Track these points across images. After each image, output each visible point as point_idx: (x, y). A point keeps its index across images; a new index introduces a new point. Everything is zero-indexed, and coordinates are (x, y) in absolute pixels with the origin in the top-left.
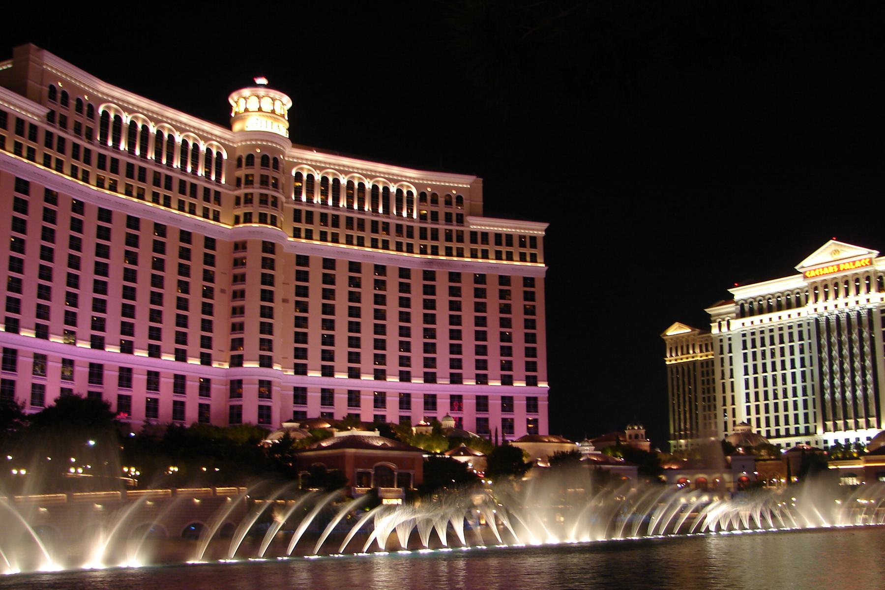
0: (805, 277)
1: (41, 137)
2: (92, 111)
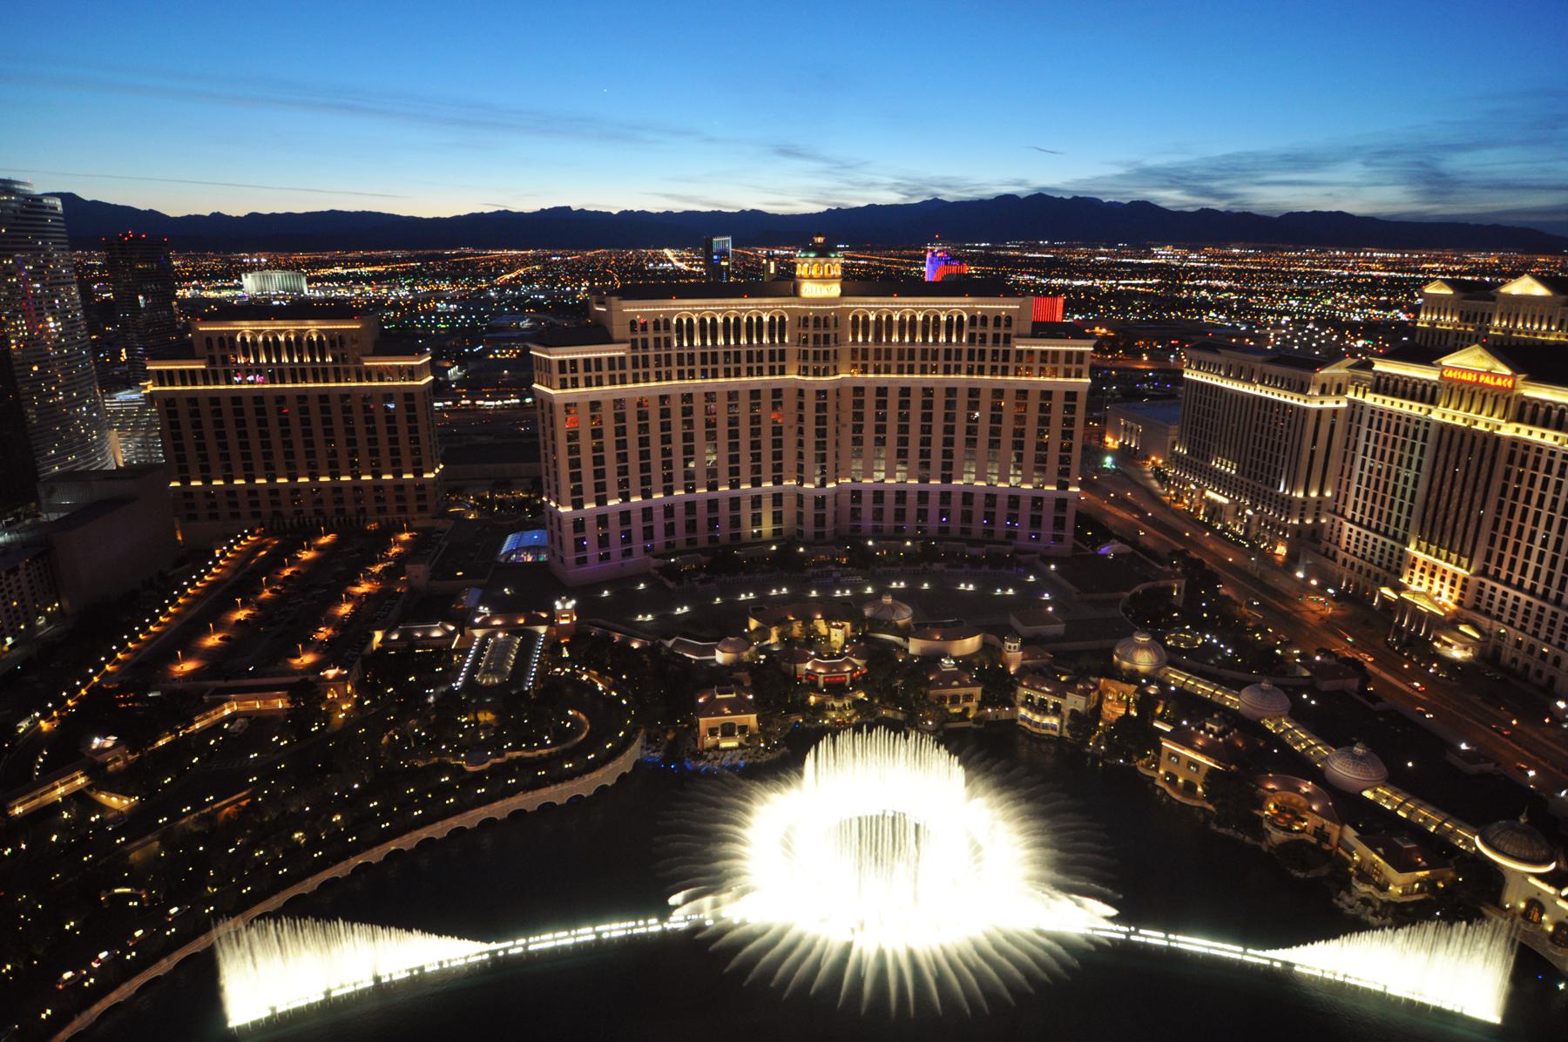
1: (629, 363)
2: (667, 322)
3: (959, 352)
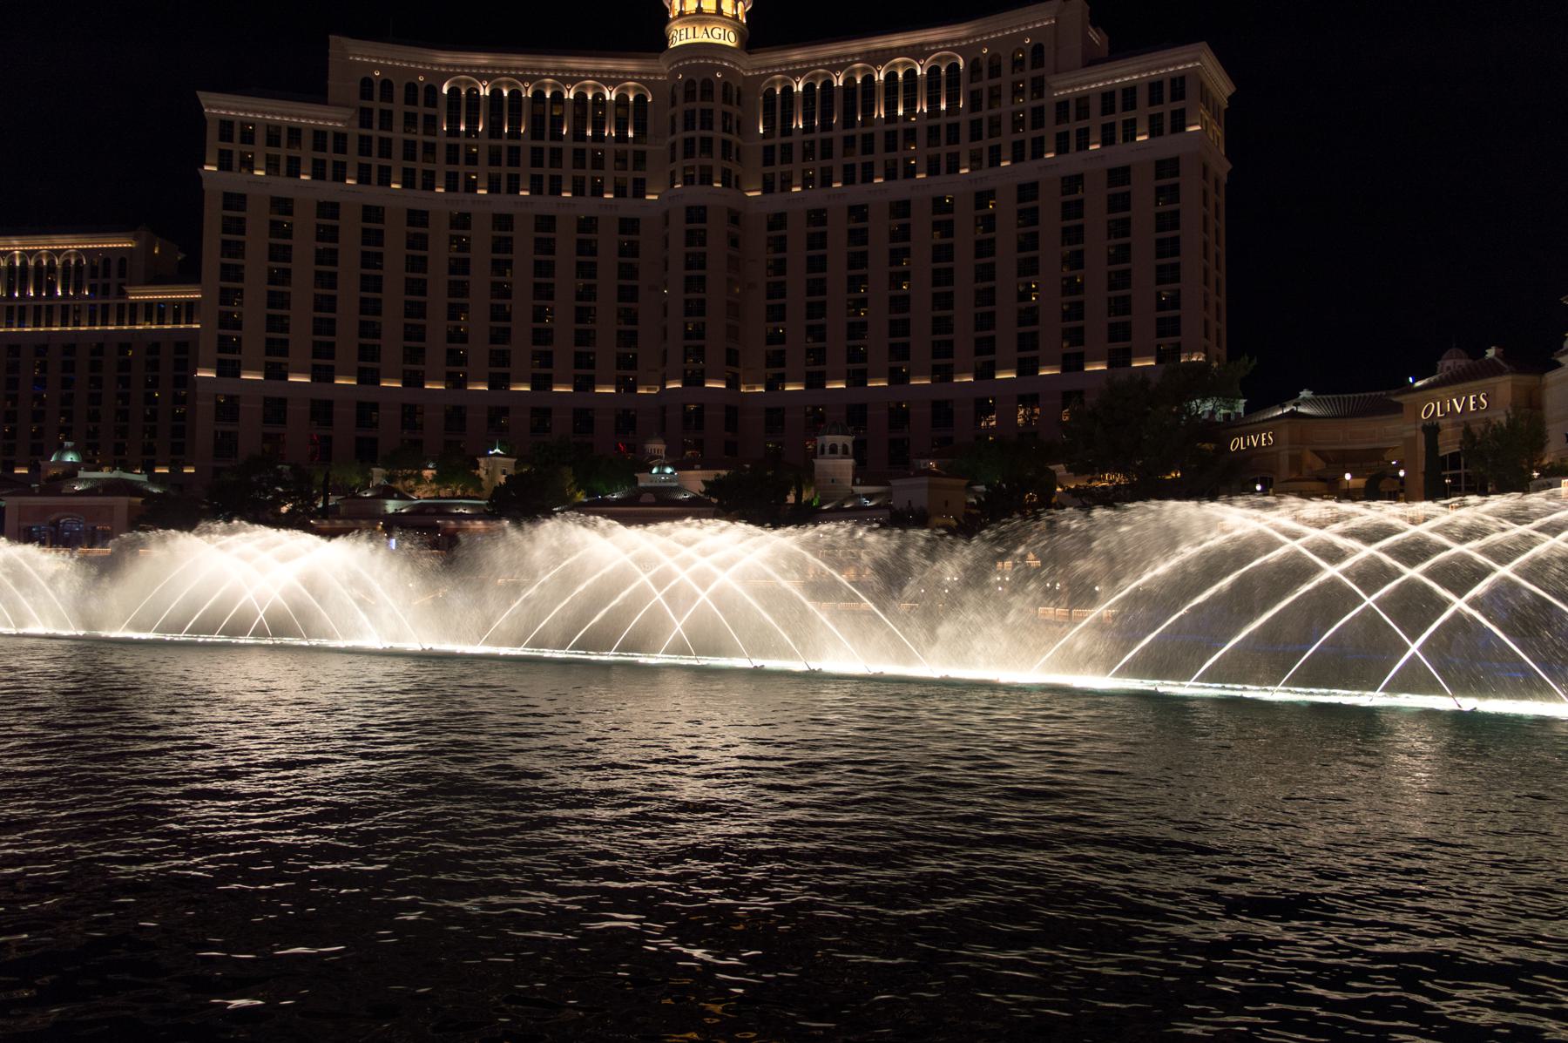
1: (353, 146)
2: (433, 91)
3: (953, 129)
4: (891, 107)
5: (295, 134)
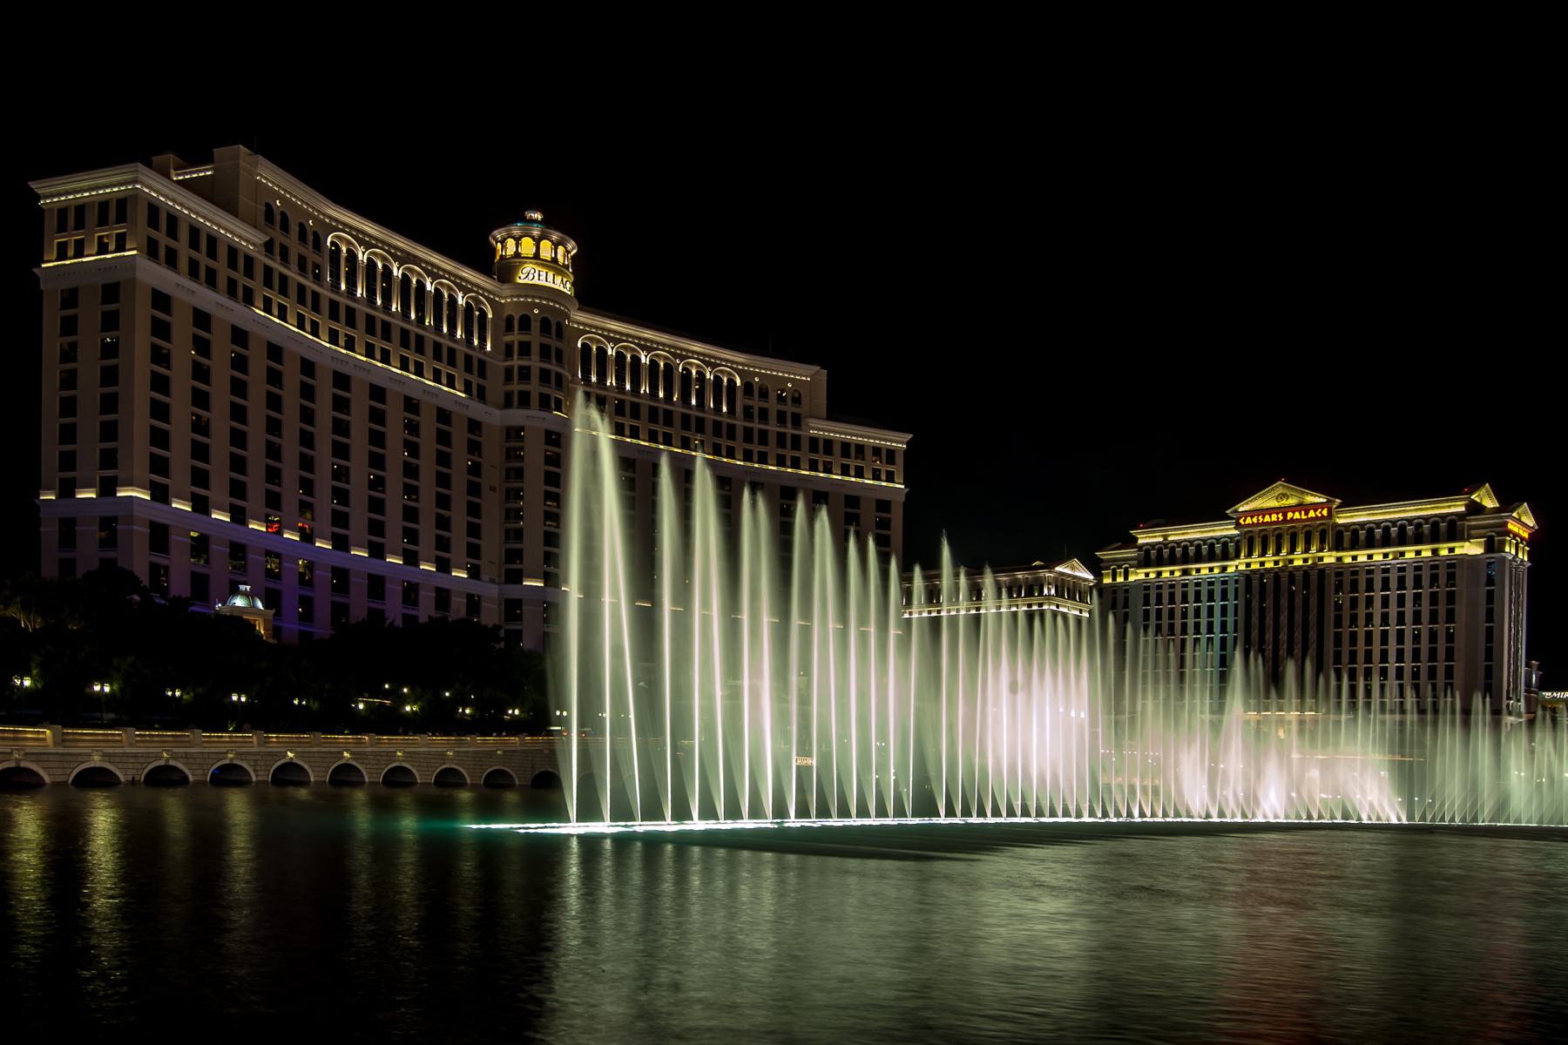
0: (1238, 525)
1: (259, 273)
4: (654, 388)
5: (213, 241)
